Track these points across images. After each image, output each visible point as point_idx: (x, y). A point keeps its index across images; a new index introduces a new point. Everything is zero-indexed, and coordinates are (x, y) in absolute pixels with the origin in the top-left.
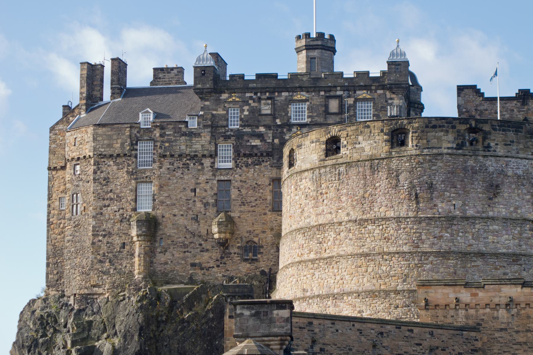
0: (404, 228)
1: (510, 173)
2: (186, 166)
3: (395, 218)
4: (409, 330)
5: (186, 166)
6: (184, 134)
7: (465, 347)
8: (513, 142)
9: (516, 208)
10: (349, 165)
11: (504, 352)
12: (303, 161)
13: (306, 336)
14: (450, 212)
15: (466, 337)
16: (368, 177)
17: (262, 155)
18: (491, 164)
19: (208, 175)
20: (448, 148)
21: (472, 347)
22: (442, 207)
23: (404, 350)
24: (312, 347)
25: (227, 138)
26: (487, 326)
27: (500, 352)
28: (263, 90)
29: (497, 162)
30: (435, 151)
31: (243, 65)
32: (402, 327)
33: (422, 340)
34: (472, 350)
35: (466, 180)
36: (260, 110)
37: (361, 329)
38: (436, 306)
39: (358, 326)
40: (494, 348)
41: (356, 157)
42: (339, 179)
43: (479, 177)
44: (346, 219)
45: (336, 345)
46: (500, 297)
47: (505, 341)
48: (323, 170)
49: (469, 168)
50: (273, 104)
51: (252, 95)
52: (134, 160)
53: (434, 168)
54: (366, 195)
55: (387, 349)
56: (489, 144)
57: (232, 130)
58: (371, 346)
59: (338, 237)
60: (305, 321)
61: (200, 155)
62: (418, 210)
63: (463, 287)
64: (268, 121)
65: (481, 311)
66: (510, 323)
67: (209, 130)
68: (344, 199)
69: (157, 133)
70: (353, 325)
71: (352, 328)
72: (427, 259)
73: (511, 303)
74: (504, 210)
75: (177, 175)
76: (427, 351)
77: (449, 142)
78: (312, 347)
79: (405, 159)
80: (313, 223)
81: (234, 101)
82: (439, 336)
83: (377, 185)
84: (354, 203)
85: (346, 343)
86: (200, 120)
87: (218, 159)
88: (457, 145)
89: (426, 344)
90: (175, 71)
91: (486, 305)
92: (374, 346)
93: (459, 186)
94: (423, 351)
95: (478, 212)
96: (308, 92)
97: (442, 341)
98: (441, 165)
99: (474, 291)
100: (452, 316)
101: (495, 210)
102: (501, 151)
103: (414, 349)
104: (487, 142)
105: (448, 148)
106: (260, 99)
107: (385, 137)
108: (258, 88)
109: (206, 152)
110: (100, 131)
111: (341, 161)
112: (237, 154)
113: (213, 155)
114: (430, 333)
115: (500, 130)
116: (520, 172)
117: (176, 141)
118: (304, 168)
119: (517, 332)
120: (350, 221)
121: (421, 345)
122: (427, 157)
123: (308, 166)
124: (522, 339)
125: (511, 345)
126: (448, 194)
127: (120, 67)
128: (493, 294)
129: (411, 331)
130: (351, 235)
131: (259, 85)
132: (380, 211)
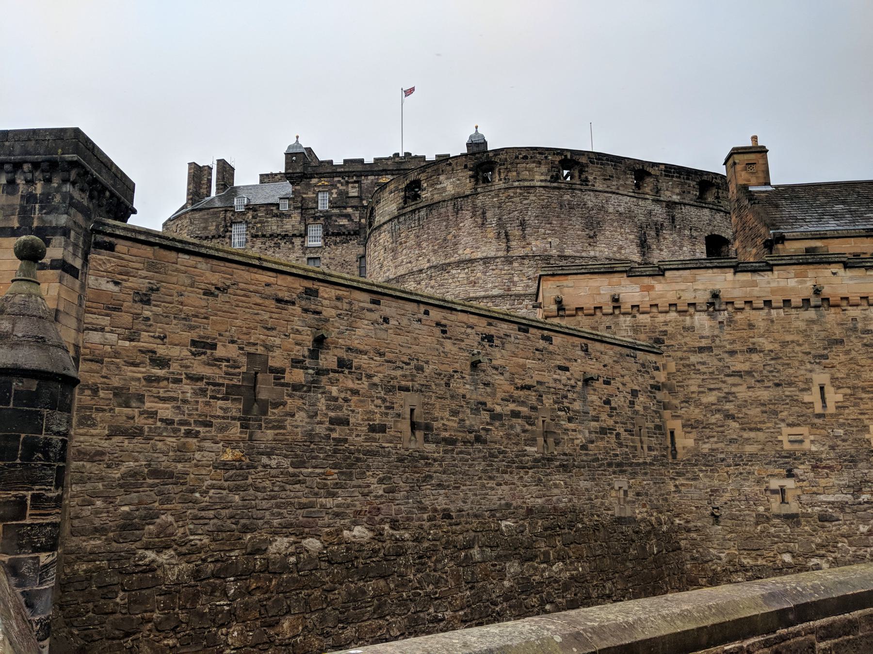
0: (493, 270)
1: (611, 210)
2: (278, 245)
3: (481, 259)
4: (544, 338)
5: (278, 245)
6: (276, 216)
7: (640, 379)
8: (612, 177)
9: (621, 248)
10: (431, 206)
11: (710, 390)
12: (381, 215)
13: (297, 324)
14: (546, 250)
15: (641, 361)
16: (451, 218)
17: (349, 234)
18: (590, 200)
19: (299, 253)
20: (541, 181)
21: (652, 382)
22: (537, 245)
23: (537, 378)
24: (314, 354)
25: (316, 218)
26: (672, 343)
27: (702, 389)
28: (349, 174)
29: (596, 197)
30: (527, 184)
31: (332, 151)
32: (531, 330)
33: (570, 360)
34: (652, 386)
35: (562, 216)
36: (347, 193)
37: (444, 322)
38: (577, 309)
39: (436, 314)
40: (691, 382)
41: (437, 198)
42: (419, 225)
43: (577, 212)
44: (428, 265)
45: (382, 355)
46: (695, 290)
47: (711, 370)
48: (402, 219)
49: (566, 203)
50: (360, 187)
51: (340, 179)
52: (228, 241)
53: (525, 202)
54: (449, 237)
55: (502, 374)
56: (586, 178)
57: (321, 212)
58: (469, 363)
59: (419, 286)
60: (297, 285)
61: (290, 234)
62: (508, 249)
63: (625, 275)
64: (355, 202)
65: (661, 318)
66: (717, 336)
67: (299, 211)
68: (424, 244)
69: (250, 215)
70: (426, 313)
71: (425, 317)
72: (521, 304)
73: (717, 302)
74: (606, 250)
75: (268, 253)
76: (580, 383)
77: (542, 174)
78: (314, 354)
79: (493, 194)
80: (391, 277)
81: (323, 185)
82: (598, 354)
83: (461, 225)
84: (436, 248)
85: (409, 351)
86: (291, 202)
87: (308, 239)
88: (552, 177)
89: (576, 369)
90: (279, 176)
91: (670, 305)
92: (475, 365)
93: (555, 222)
94: (572, 382)
95: (578, 251)
96: (393, 175)
97: (605, 366)
98: (534, 198)
99: (647, 281)
100: (609, 327)
101: (597, 249)
102: (599, 186)
103: (555, 376)
104: (583, 177)
105: (541, 181)
106: (347, 183)
107: (471, 173)
108: (346, 172)
109: (296, 232)
110: (197, 215)
111: (421, 205)
112: (326, 235)
113: (303, 235)
114: (582, 347)
115: (597, 163)
116: (621, 209)
117: (267, 222)
118: (383, 220)
119: (732, 353)
120: (431, 267)
121: (566, 369)
122: (518, 191)
123: (387, 218)
124: (743, 365)
125: (722, 376)
126: (543, 230)
127: (226, 170)
128: (683, 286)
129: (548, 339)
130: (433, 282)
131: (347, 170)
132: (465, 253)
